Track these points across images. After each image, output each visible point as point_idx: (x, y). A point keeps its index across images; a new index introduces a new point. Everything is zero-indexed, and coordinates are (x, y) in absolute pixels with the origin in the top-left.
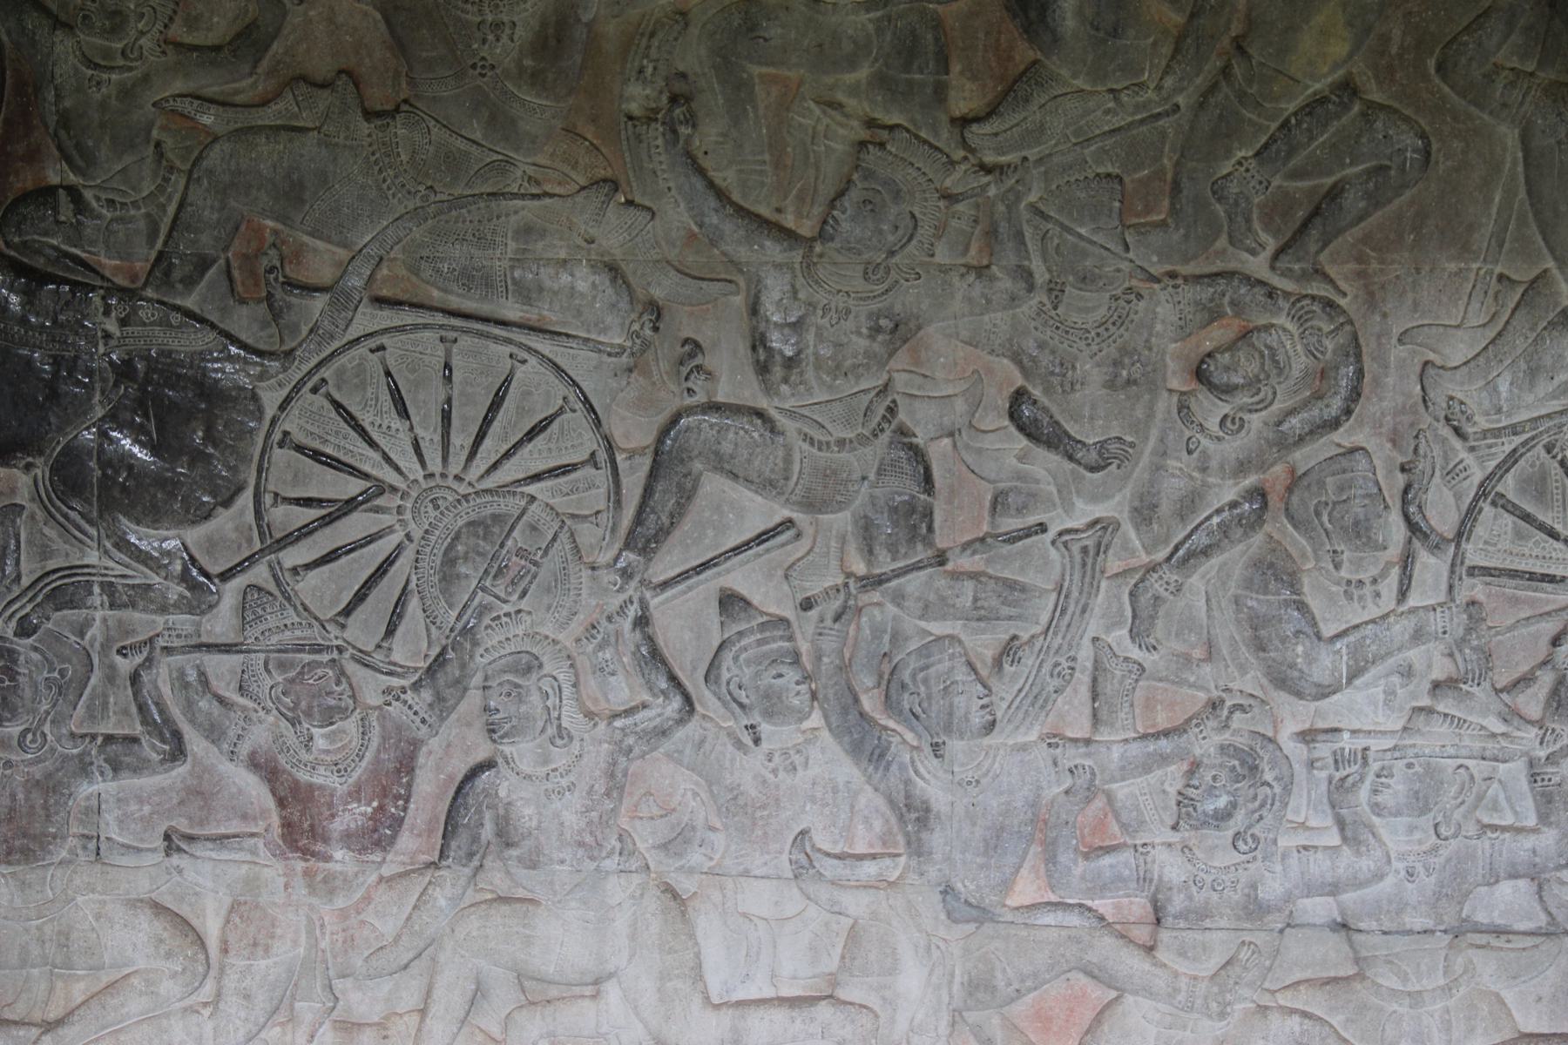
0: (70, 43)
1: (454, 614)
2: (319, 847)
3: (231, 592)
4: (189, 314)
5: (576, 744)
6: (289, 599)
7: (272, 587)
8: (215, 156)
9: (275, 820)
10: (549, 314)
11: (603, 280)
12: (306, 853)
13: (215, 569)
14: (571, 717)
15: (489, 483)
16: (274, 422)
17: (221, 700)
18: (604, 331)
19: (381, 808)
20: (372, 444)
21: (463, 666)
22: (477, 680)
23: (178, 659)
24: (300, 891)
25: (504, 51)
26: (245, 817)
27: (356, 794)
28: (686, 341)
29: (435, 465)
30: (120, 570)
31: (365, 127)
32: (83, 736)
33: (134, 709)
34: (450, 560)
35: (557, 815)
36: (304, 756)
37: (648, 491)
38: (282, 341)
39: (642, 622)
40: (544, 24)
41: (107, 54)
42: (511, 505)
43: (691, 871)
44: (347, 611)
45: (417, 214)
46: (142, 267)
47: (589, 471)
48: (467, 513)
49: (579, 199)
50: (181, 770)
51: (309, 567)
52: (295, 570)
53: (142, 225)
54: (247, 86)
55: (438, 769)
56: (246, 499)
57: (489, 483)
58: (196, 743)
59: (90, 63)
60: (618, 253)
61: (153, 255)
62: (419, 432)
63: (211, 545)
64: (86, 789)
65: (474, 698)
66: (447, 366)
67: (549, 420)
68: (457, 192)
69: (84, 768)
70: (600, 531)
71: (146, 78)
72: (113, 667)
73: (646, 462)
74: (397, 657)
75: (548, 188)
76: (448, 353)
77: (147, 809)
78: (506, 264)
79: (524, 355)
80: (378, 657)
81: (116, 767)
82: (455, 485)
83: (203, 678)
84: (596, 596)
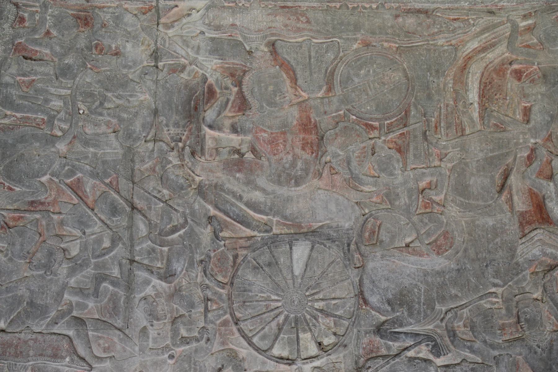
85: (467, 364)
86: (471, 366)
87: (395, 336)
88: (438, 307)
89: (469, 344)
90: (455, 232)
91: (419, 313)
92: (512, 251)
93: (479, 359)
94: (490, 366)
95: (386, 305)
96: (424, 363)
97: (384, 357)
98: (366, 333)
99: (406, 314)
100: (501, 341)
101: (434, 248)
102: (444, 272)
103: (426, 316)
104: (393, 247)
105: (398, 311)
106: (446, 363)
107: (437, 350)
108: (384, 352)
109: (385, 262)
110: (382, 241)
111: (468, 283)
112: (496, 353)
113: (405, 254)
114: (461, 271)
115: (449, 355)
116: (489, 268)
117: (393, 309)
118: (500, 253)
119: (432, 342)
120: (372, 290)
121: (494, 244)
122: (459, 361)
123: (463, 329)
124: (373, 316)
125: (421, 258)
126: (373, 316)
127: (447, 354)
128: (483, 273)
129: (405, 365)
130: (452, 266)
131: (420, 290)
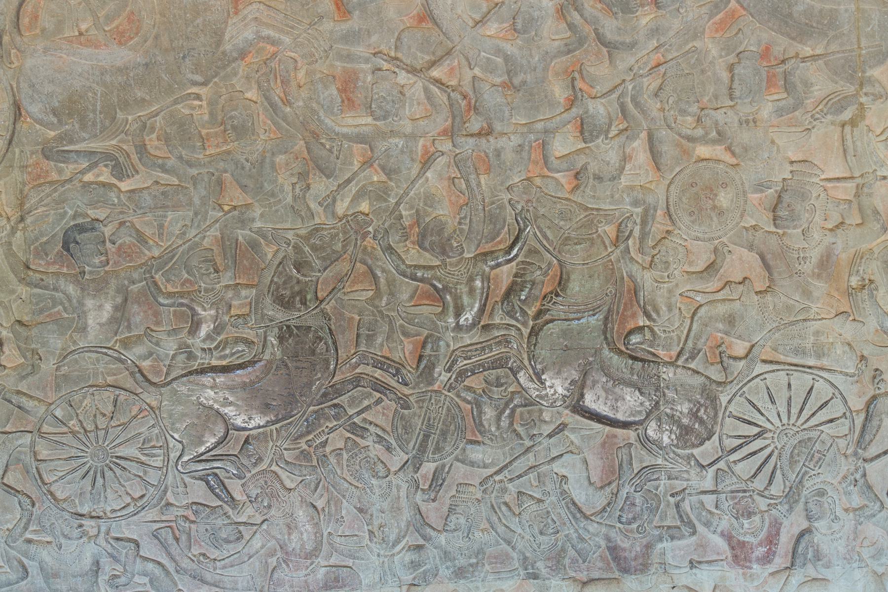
0: (649, 274)
1: (795, 476)
2: (748, 564)
3: (711, 471)
4: (693, 370)
5: (842, 521)
6: (733, 473)
7: (726, 469)
8: (702, 312)
9: (729, 554)
10: (825, 362)
11: (847, 348)
12: (743, 567)
13: (705, 464)
14: (839, 512)
15: (805, 426)
16: (726, 408)
17: (710, 512)
18: (847, 368)
19: (770, 549)
20: (762, 414)
21: (799, 495)
22: (803, 500)
23: (694, 499)
24: (741, 580)
25: (807, 268)
26: (718, 554)
27: (760, 544)
28: (877, 370)
29: (785, 421)
30: (671, 466)
31: (756, 298)
32: (659, 527)
33: (677, 517)
34: (792, 456)
35: (836, 548)
36: (741, 531)
37: (864, 426)
38: (726, 378)
39: (864, 475)
40: (822, 257)
41: (662, 277)
42: (814, 434)
43: (882, 565)
44: (755, 475)
45: (778, 329)
46: (674, 353)
47: (843, 420)
48: (799, 437)
49: (836, 319)
50: (694, 538)
51: (739, 461)
52: (734, 462)
53: (675, 338)
54: (713, 285)
55: (788, 532)
56: (716, 438)
57: (805, 426)
58: (700, 528)
59: (657, 281)
60: (849, 339)
61: (679, 349)
62: (779, 409)
63: (703, 454)
64: (660, 546)
65: (801, 506)
66: (789, 385)
67: (826, 403)
68: (791, 319)
69: (661, 539)
70: (846, 442)
71: (677, 285)
72: (668, 501)
73: (863, 416)
74: (772, 493)
75: (823, 316)
76: (789, 379)
77: (682, 552)
78: (810, 345)
79: (818, 378)
80: (766, 493)
81: (672, 538)
82: (794, 428)
83: (702, 503)
84: (845, 466)
85: (156, 187)
86: (162, 189)
87: (64, 156)
88: (120, 115)
89: (160, 161)
90: (143, 13)
91: (94, 124)
92: (218, 36)
93: (175, 179)
94: (186, 188)
95: (51, 116)
96: (102, 189)
97: (51, 183)
98: (32, 153)
99: (77, 126)
100: (201, 156)
101: (115, 36)
102: (127, 68)
103: (104, 129)
104: (61, 36)
105: (66, 124)
106: (133, 188)
107: (120, 172)
108: (54, 176)
109: (49, 58)
110: (43, 30)
111: (159, 81)
112: (194, 172)
113: (75, 46)
114: (151, 66)
115: (137, 177)
116: (187, 60)
117: (60, 121)
118: (202, 39)
119: (111, 161)
120: (32, 97)
121: (194, 27)
122: (149, 183)
123: (156, 143)
124: (37, 131)
125: (97, 51)
126: (37, 131)
127: (133, 176)
128: (179, 68)
129: (78, 191)
130: (138, 60)
131: (95, 94)
